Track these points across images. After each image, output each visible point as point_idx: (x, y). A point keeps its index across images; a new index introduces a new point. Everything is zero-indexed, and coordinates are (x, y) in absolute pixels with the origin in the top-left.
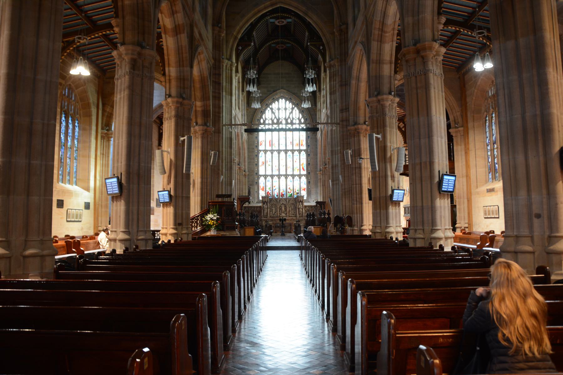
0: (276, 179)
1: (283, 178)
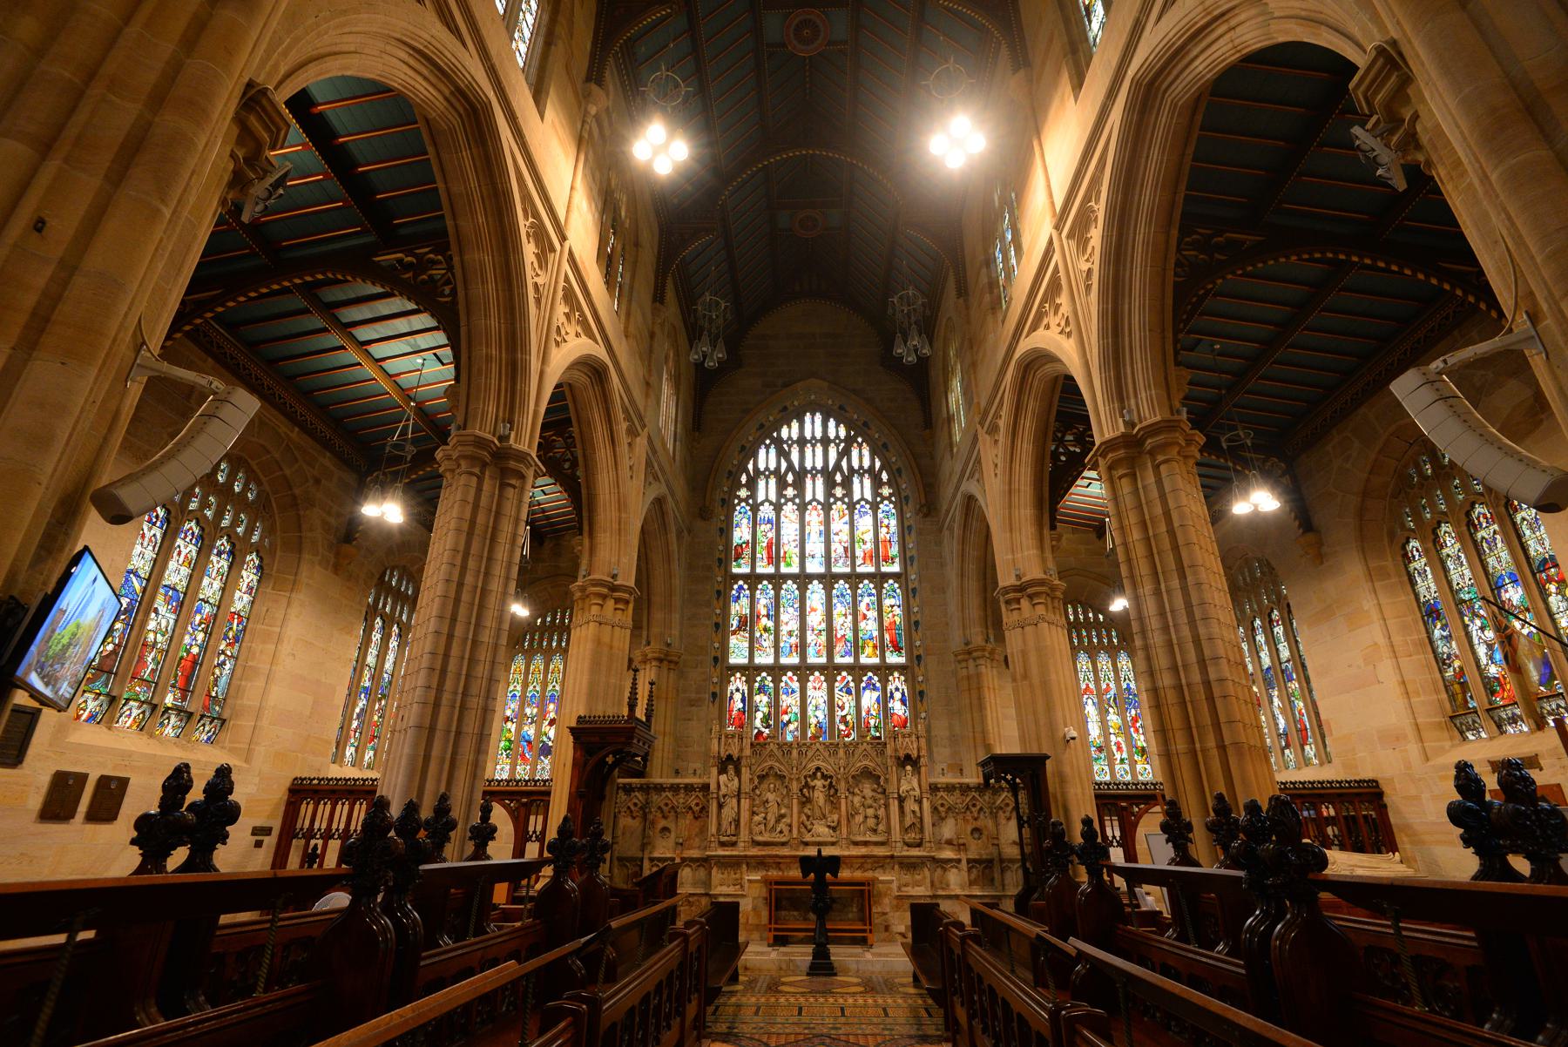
0: (790, 681)
1: (816, 680)
